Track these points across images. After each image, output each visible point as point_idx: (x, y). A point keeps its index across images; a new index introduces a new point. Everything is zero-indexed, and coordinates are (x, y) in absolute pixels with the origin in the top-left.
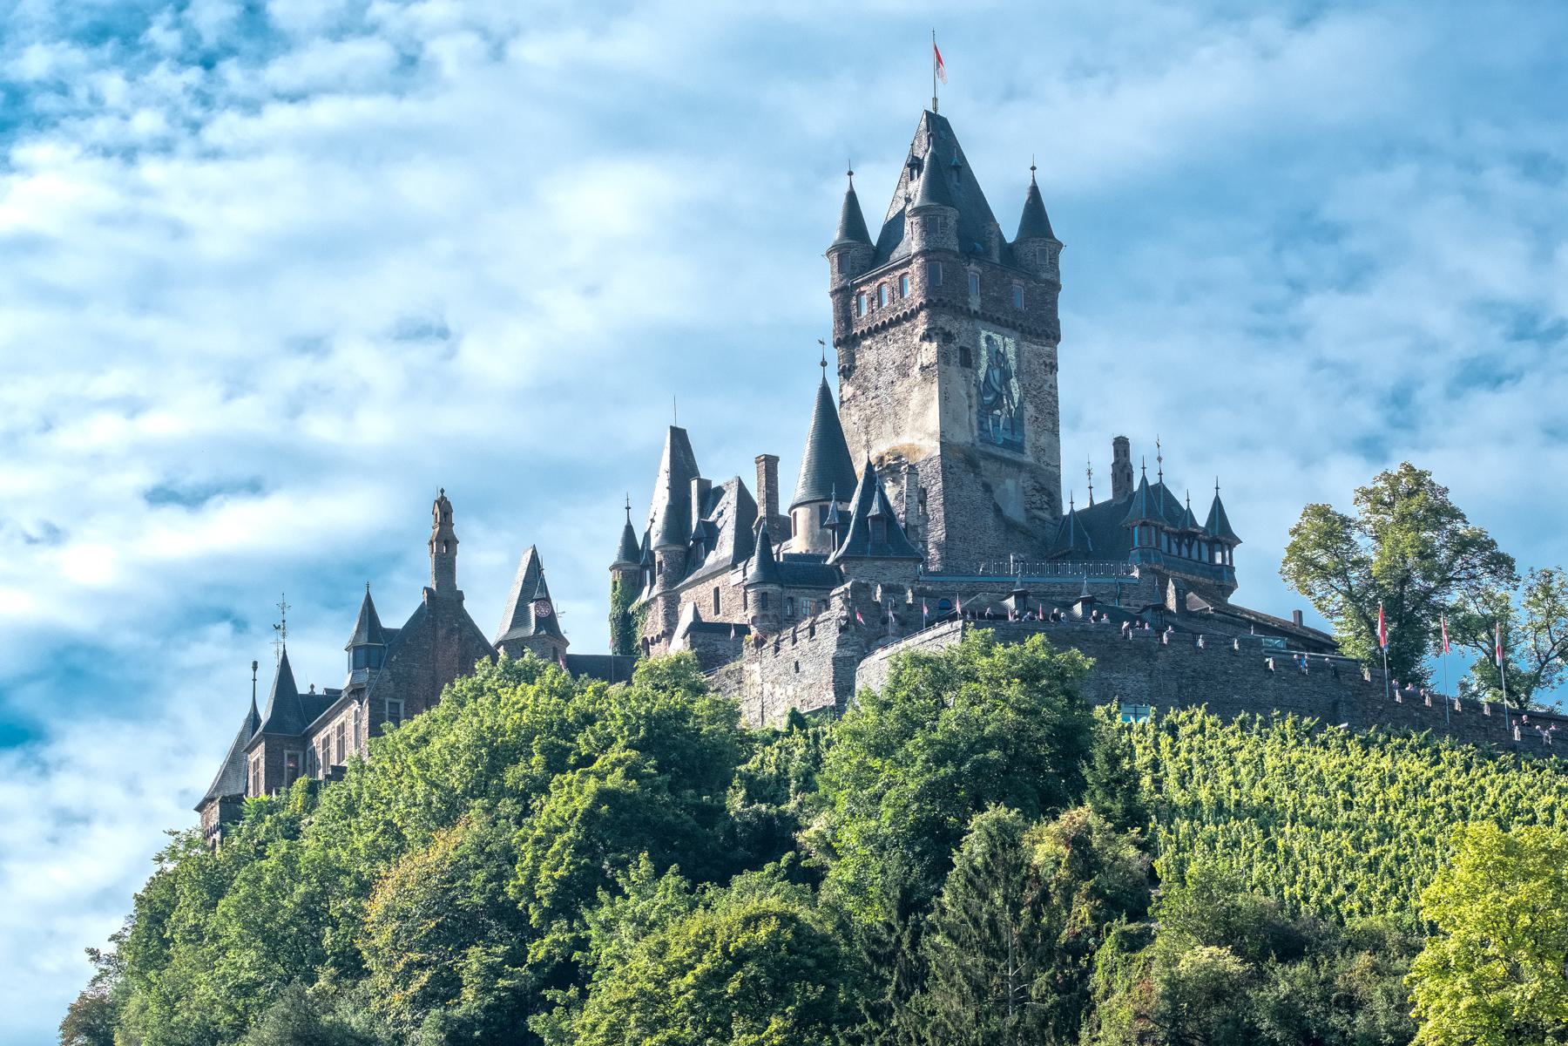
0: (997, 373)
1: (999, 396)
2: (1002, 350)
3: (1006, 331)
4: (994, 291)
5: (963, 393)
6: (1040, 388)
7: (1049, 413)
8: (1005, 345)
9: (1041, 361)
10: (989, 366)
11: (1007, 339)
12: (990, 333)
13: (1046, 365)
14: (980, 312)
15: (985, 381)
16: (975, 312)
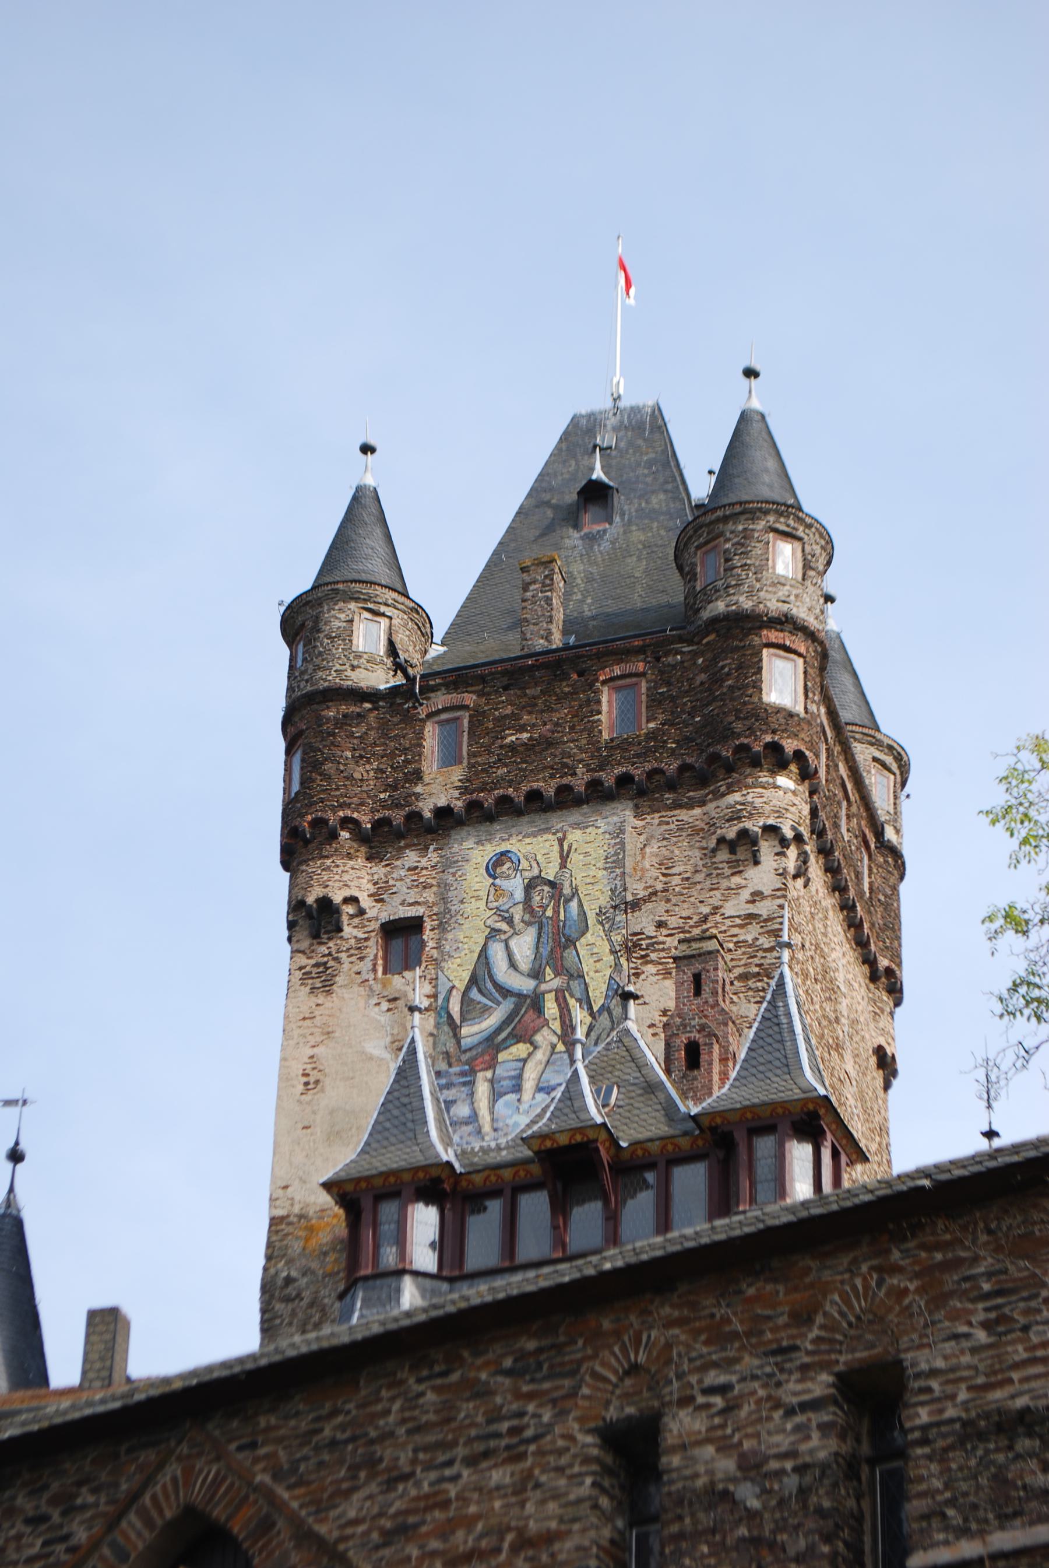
0: (524, 946)
1: (536, 1002)
2: (550, 874)
3: (558, 821)
4: (522, 729)
5: (377, 1047)
6: (705, 919)
7: (744, 977)
8: (564, 859)
9: (712, 843)
10: (494, 933)
11: (575, 836)
12: (504, 847)
13: (732, 846)
14: (458, 805)
15: (474, 980)
16: (443, 813)
